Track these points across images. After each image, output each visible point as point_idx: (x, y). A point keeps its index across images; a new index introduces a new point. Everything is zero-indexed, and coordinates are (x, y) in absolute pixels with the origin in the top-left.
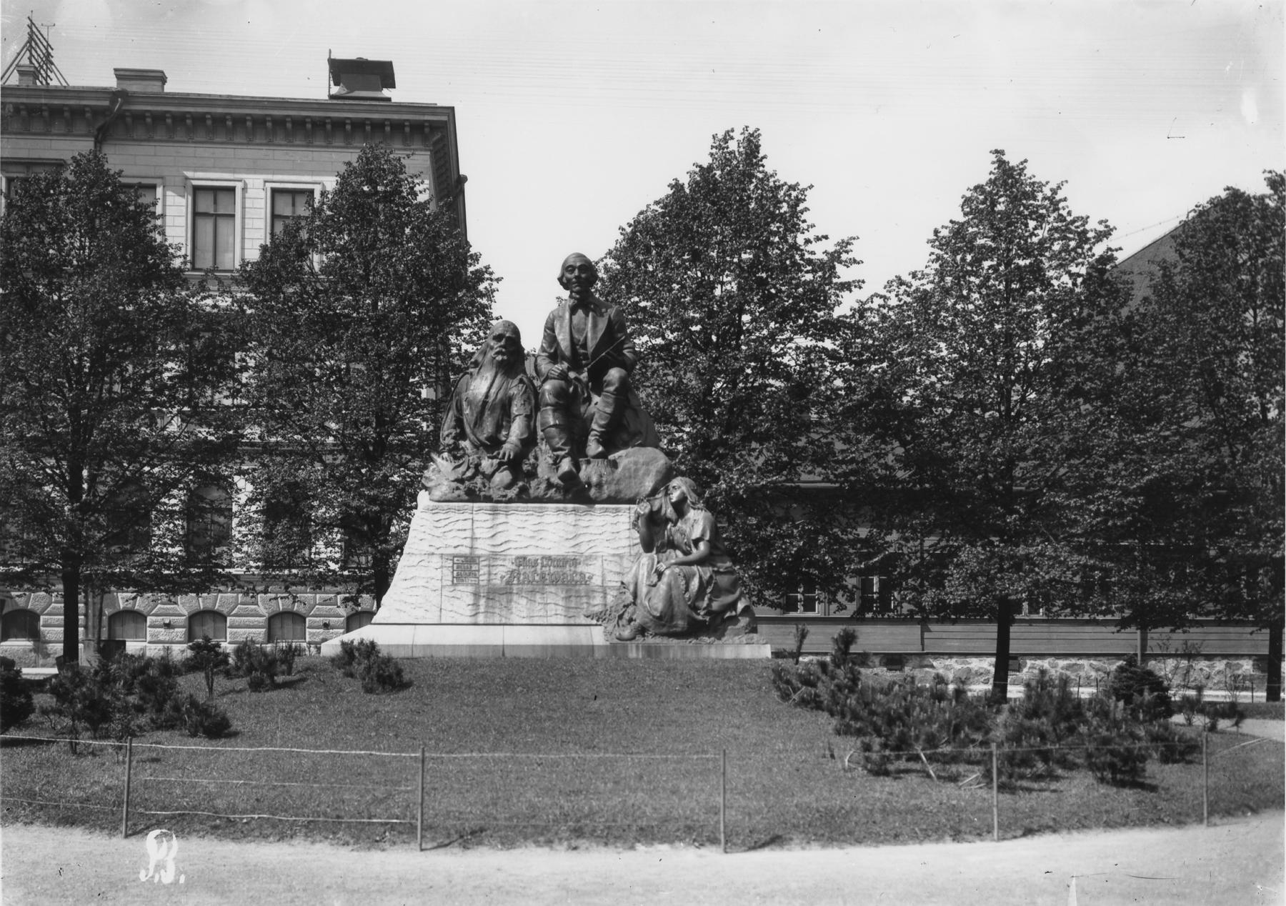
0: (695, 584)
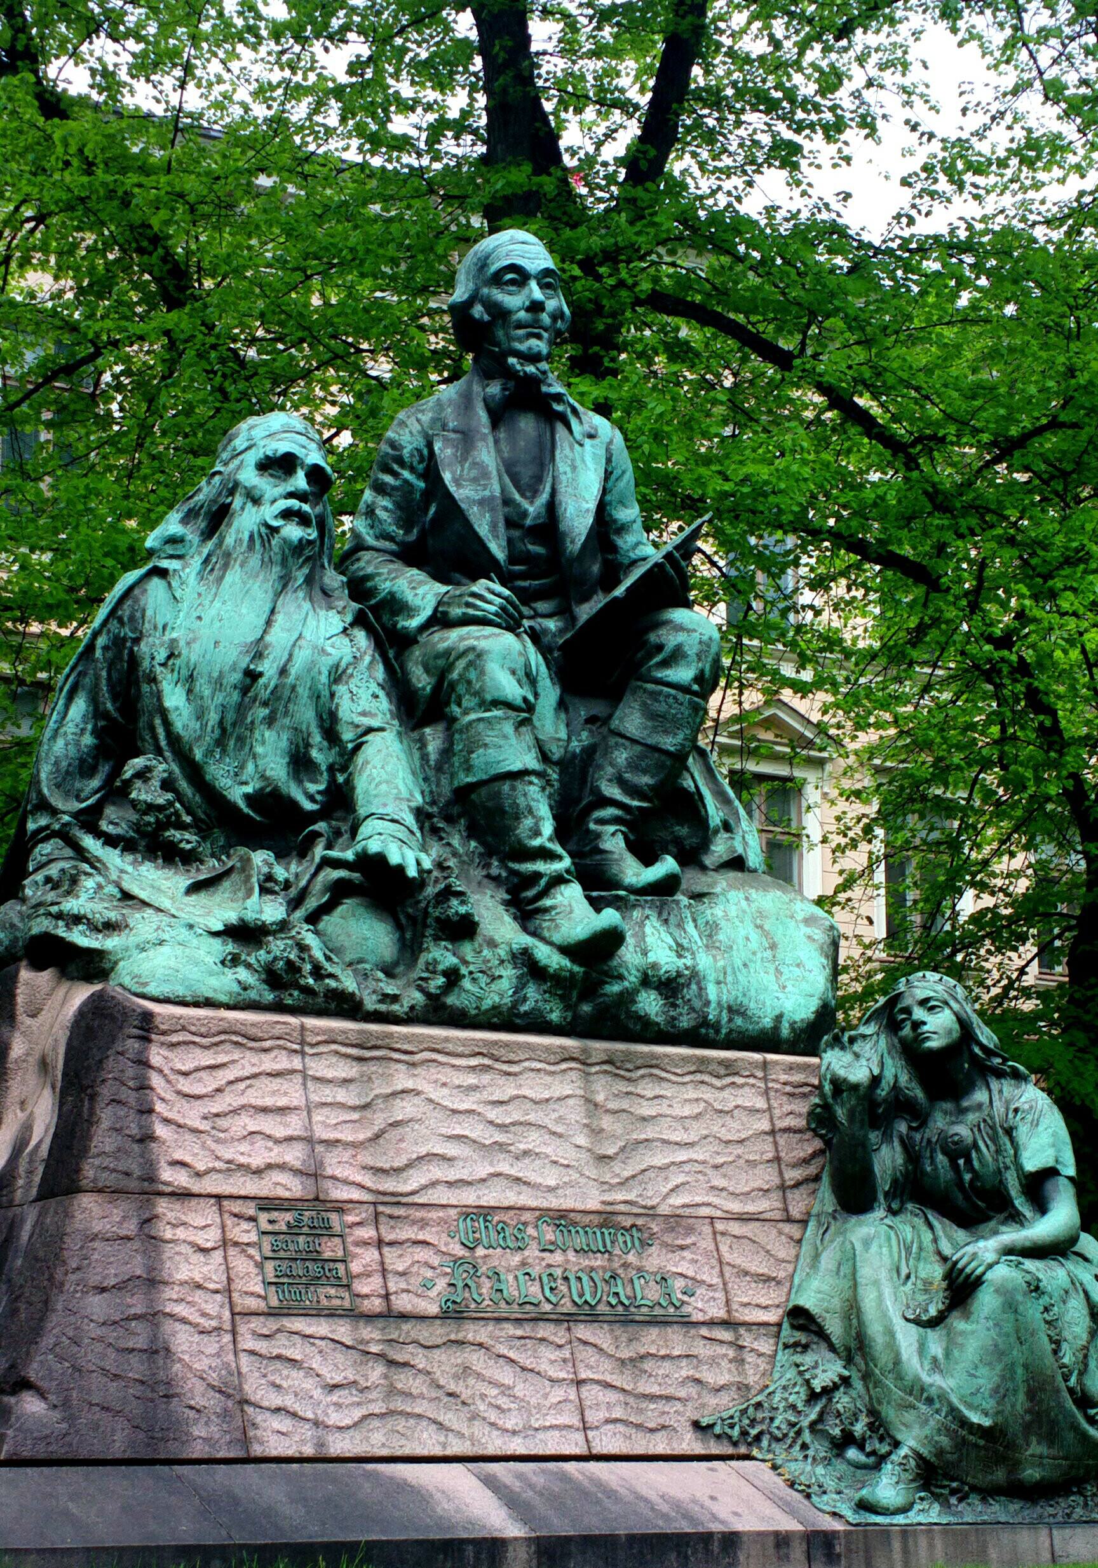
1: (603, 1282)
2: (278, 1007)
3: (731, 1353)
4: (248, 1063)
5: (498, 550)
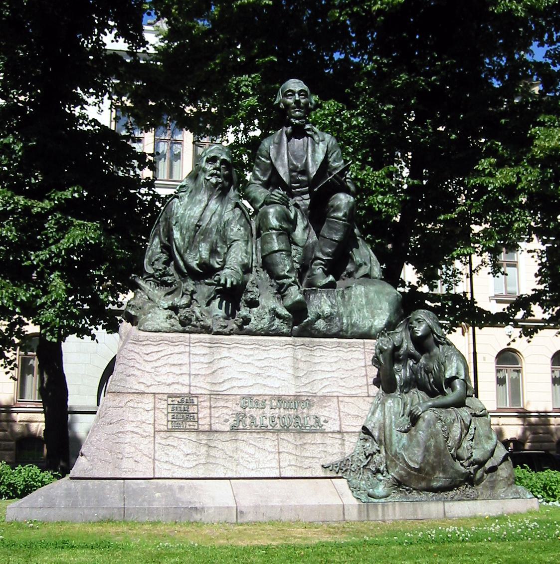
0: (456, 431)
1: (294, 418)
2: (184, 332)
3: (340, 442)
4: (170, 349)
5: (286, 179)
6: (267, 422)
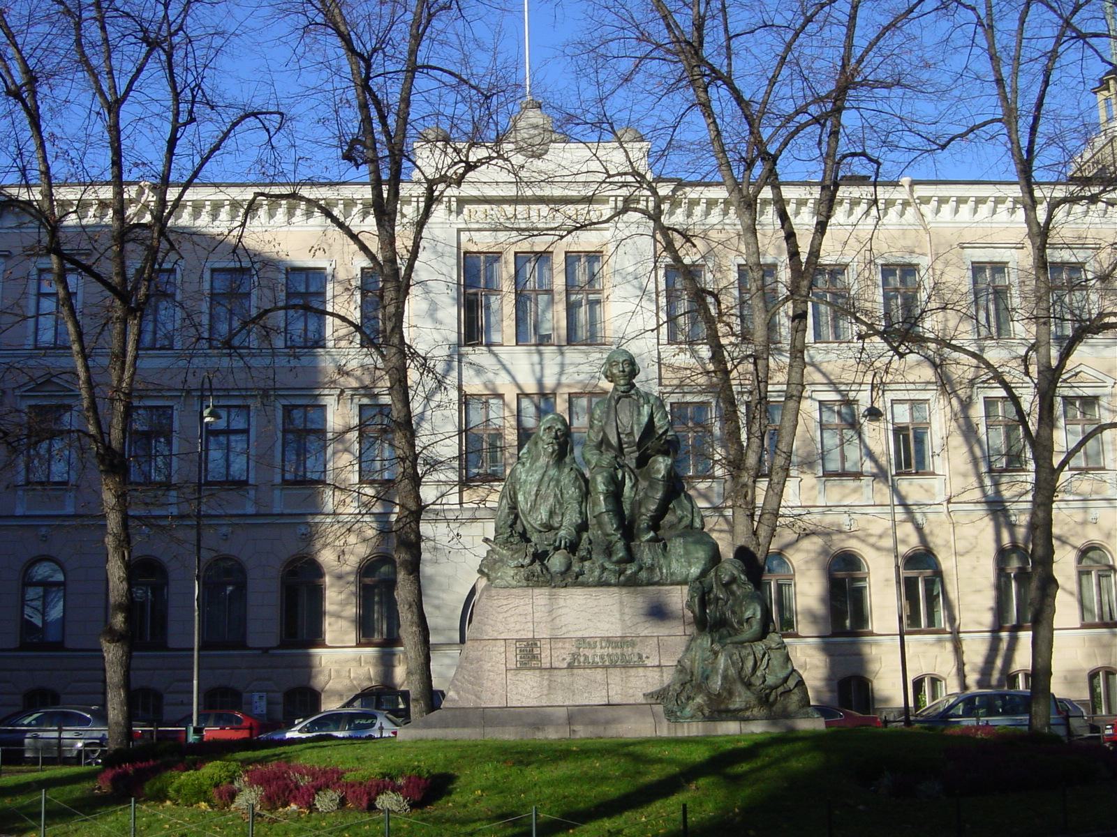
6: (597, 659)
